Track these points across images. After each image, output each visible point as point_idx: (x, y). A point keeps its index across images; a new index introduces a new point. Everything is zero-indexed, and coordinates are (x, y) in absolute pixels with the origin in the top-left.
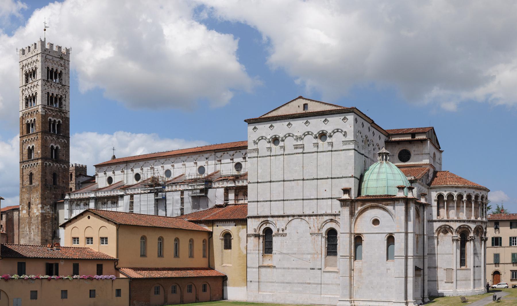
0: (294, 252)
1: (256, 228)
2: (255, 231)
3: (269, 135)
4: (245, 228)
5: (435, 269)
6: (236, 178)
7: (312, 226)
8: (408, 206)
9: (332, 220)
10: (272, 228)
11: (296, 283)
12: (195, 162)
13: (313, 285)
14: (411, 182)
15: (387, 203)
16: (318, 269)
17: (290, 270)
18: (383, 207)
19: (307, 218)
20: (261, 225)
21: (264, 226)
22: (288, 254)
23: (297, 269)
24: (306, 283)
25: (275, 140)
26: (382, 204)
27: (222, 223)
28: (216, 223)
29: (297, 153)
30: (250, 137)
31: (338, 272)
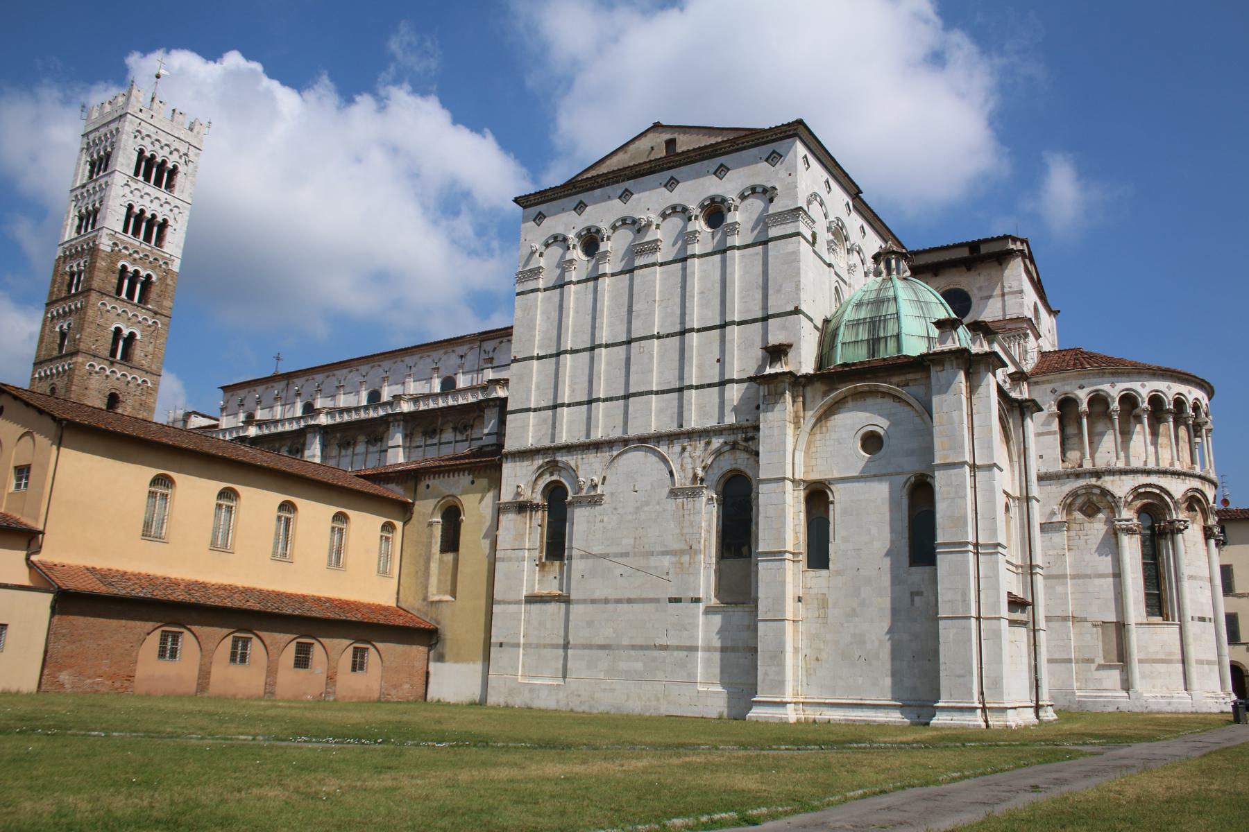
0: (623, 551)
5: (1064, 623)
9: (734, 446)
13: (676, 653)
17: (610, 607)
18: (891, 391)
21: (547, 479)
23: (630, 601)
24: (655, 647)
26: (891, 384)
27: (439, 477)
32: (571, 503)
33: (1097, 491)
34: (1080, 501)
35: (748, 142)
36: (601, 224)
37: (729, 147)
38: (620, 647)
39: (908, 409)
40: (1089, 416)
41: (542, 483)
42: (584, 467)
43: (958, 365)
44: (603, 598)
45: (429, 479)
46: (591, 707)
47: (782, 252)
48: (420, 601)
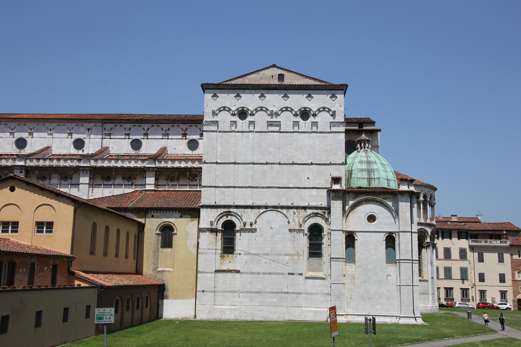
1: (213, 220)
2: (212, 223)
3: (235, 106)
7: (291, 220)
9: (316, 215)
10: (235, 222)
13: (292, 295)
16: (299, 273)
17: (260, 276)
18: (381, 201)
19: (284, 211)
20: (220, 216)
21: (225, 219)
22: (258, 255)
23: (270, 274)
25: (243, 114)
28: (151, 213)
30: (207, 106)
31: (325, 278)
32: (238, 231)
35: (322, 87)
37: (314, 87)
38: (265, 293)
42: (245, 216)
43: (409, 196)
44: (257, 272)
45: (154, 213)
46: (252, 317)
47: (337, 138)
48: (152, 271)
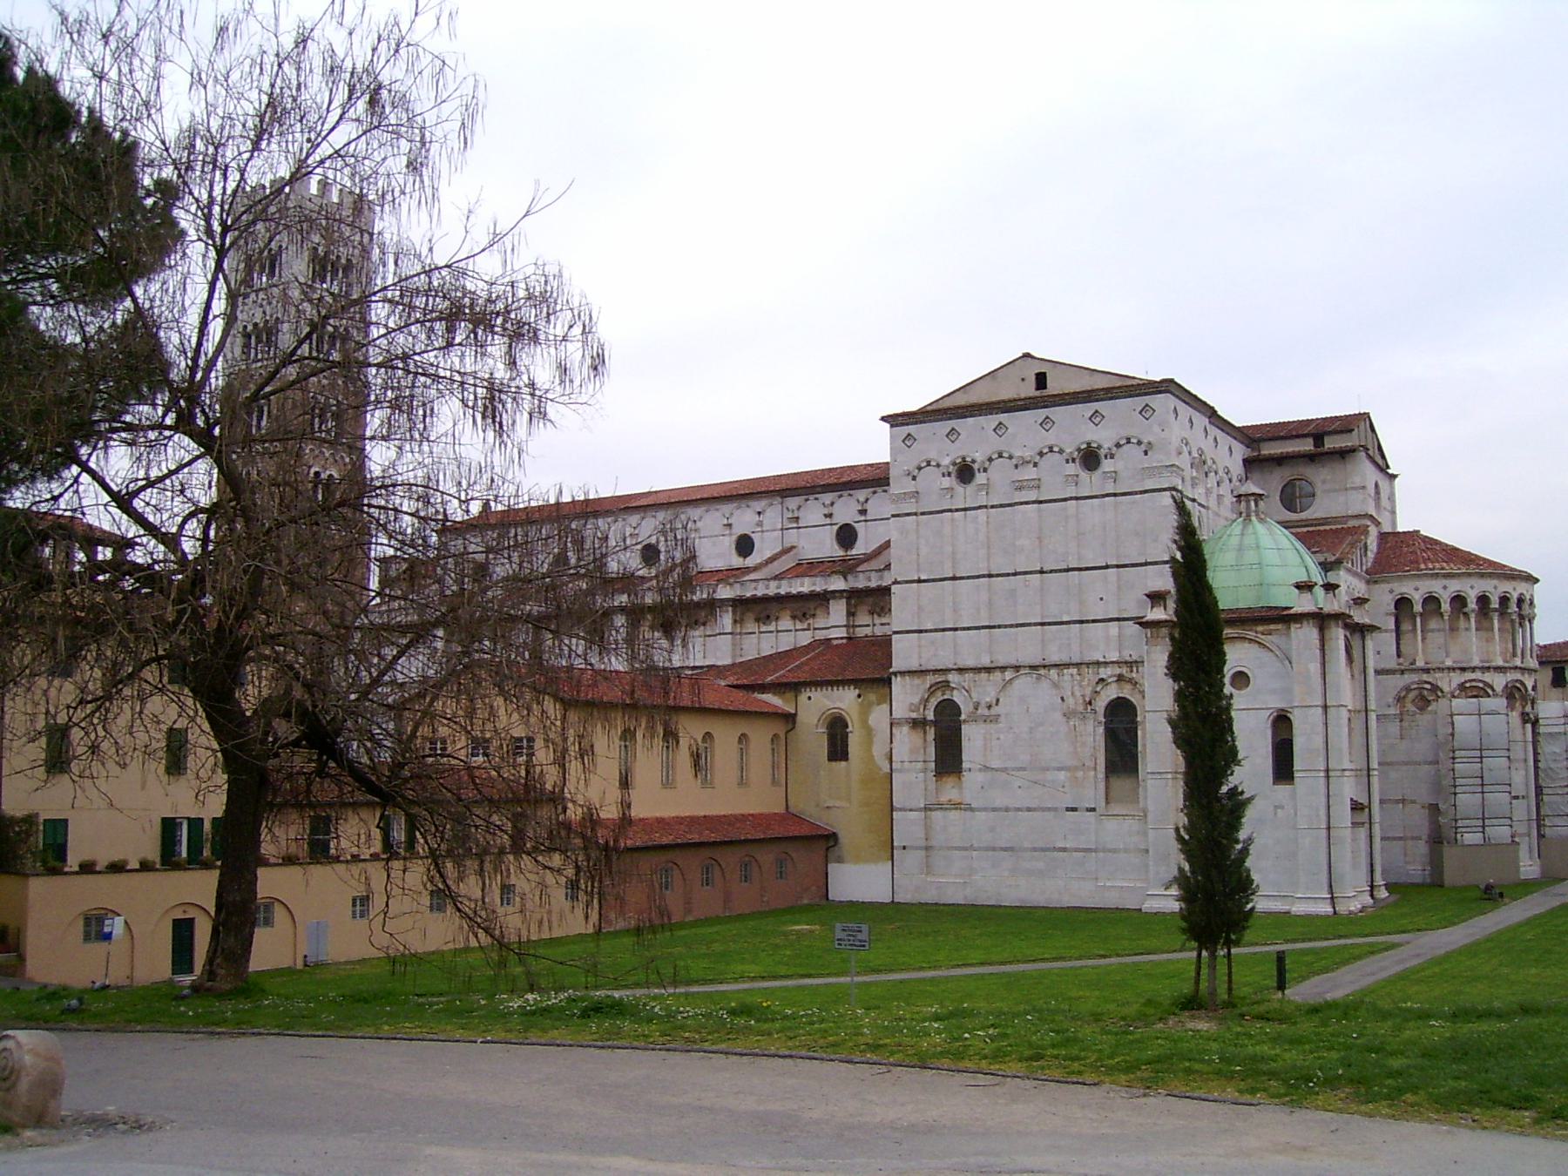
1: (916, 700)
4: (885, 702)
6: (846, 567)
8: (1327, 637)
9: (1120, 678)
11: (1026, 850)
12: (726, 522)
14: (1326, 567)
15: (1266, 627)
19: (1053, 672)
21: (939, 697)
22: (1004, 770)
23: (1029, 809)
24: (1055, 849)
29: (1022, 503)
33: (1428, 686)
34: (1412, 695)
36: (977, 454)
39: (1271, 653)
40: (1421, 615)
41: (933, 702)
